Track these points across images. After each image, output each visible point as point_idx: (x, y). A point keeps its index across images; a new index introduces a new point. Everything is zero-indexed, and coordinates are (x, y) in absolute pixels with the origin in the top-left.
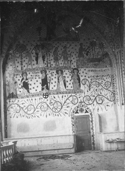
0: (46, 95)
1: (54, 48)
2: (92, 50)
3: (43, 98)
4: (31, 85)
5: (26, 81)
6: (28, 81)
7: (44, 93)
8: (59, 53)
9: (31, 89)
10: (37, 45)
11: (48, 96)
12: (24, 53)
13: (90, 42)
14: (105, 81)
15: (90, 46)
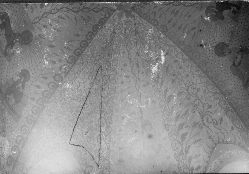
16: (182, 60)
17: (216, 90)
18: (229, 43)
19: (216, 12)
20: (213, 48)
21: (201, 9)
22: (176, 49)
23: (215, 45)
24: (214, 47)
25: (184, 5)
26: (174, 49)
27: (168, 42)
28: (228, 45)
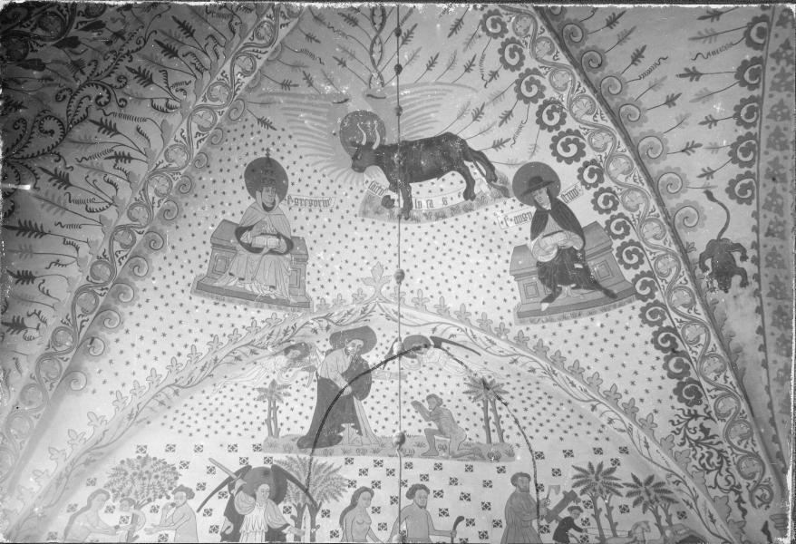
1: (352, 491)
2: (596, 516)
8: (376, 520)
10: (245, 471)
12: (155, 510)
13: (577, 469)
15: (577, 490)
16: (228, 73)
17: (156, 204)
18: (293, 198)
19: (370, 144)
20: (265, 152)
21: (368, 96)
22: (263, 50)
23: (275, 156)
24: (268, 155)
25: (374, 42)
26: (263, 42)
27: (287, 21)
28: (287, 198)
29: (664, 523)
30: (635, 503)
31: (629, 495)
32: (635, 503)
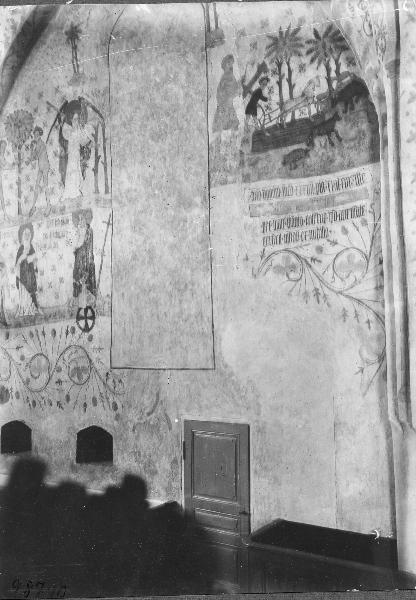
0: (86, 318)
3: (77, 329)
4: (42, 274)
5: (30, 259)
6: (36, 260)
7: (80, 309)
9: (41, 290)
11: (93, 318)
14: (337, 249)
29: (333, 74)
30: (312, 61)
31: (308, 53)
32: (312, 61)
